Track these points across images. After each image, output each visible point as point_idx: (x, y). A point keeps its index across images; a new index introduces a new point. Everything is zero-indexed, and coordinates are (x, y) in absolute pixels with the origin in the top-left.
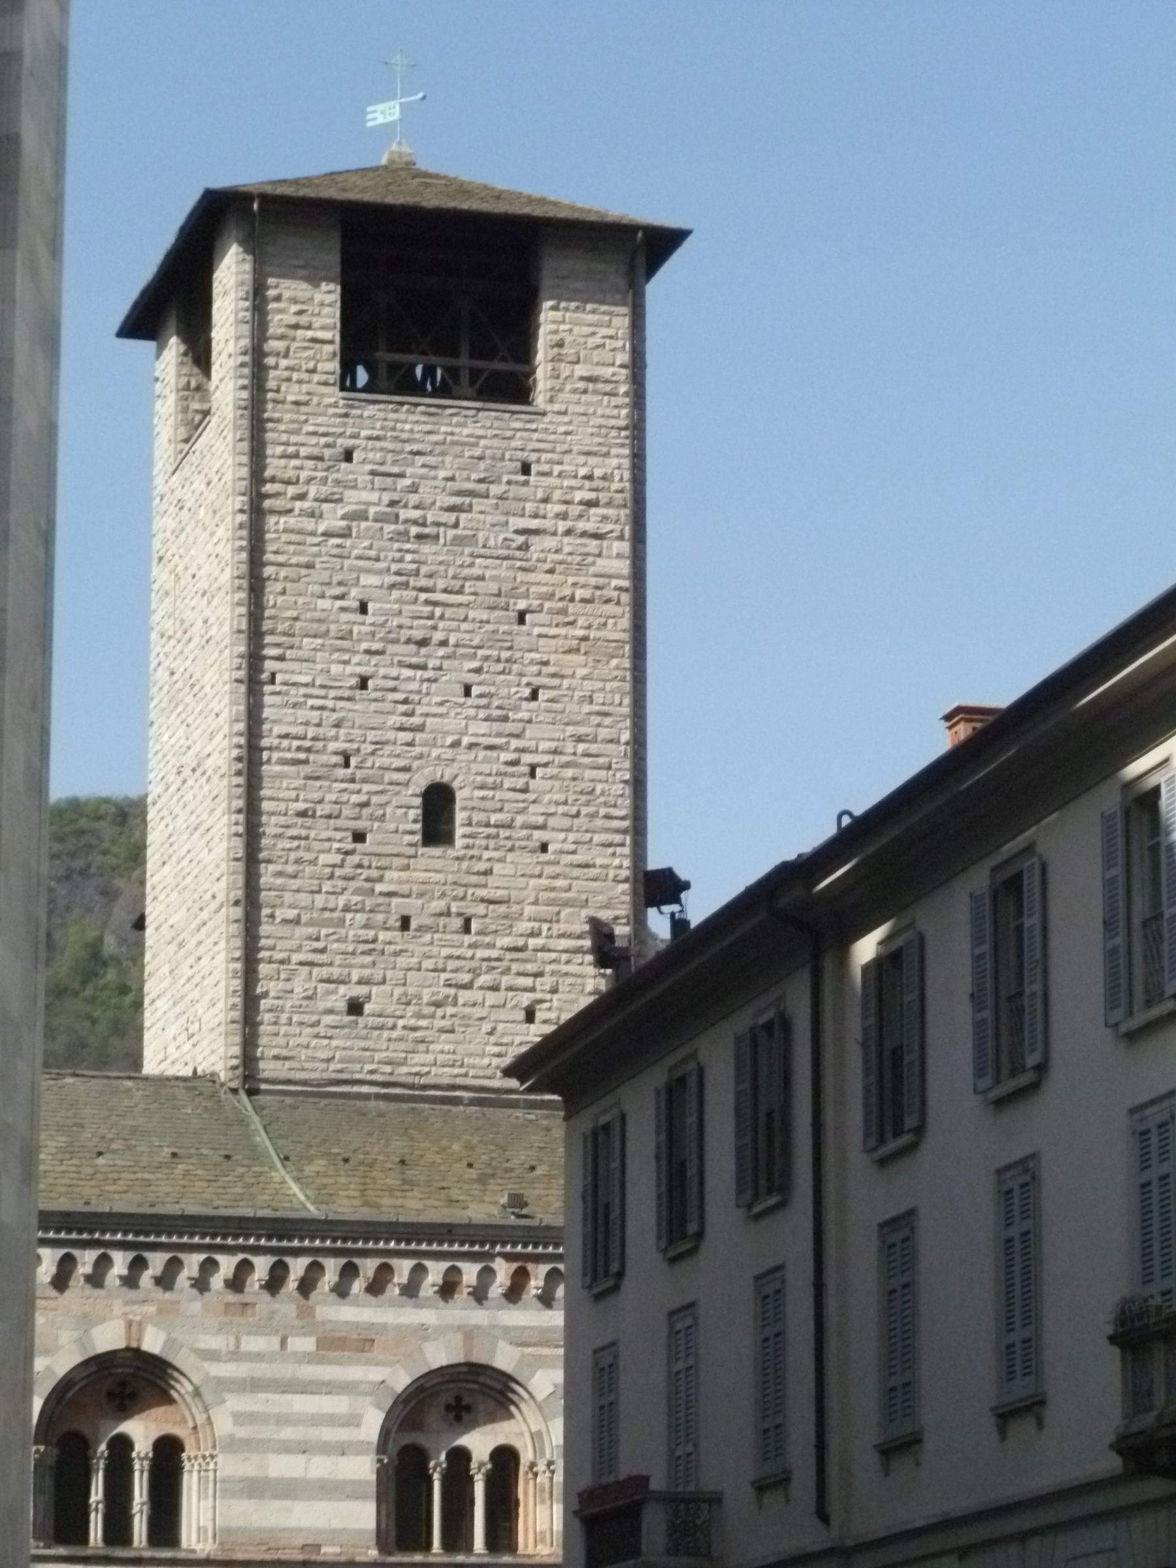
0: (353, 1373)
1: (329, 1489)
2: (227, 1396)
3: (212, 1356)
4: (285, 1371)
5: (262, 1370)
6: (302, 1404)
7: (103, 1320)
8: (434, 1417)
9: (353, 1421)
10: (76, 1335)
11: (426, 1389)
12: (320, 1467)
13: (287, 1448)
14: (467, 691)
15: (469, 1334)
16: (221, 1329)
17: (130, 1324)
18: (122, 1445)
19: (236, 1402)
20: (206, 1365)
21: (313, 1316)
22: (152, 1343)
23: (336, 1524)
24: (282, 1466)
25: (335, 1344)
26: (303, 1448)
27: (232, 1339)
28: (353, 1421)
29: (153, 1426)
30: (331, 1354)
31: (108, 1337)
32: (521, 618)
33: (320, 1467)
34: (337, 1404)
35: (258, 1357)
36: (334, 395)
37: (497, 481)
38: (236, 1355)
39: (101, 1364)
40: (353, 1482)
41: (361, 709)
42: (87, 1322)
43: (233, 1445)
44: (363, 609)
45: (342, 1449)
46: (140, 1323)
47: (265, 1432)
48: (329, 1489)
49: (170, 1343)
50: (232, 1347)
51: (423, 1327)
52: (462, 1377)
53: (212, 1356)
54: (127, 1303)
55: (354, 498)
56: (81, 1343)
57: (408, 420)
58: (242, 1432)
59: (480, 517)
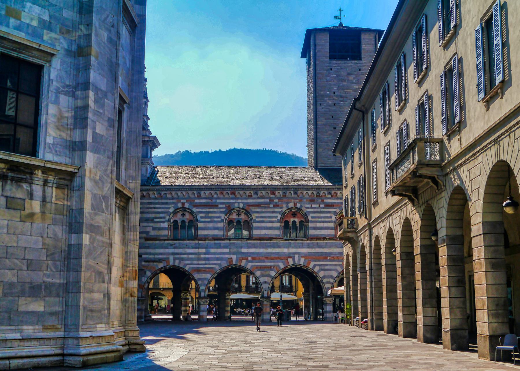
4: (319, 210)
5: (316, 210)
6: (322, 215)
7: (290, 203)
9: (331, 217)
12: (326, 225)
13: (320, 222)
16: (309, 204)
17: (294, 203)
18: (294, 222)
19: (312, 215)
22: (298, 206)
23: (329, 234)
24: (319, 225)
25: (328, 206)
28: (331, 217)
31: (291, 205)
33: (326, 225)
34: (328, 215)
35: (315, 208)
36: (328, 59)
37: (355, 71)
38: (312, 208)
39: (291, 209)
41: (333, 108)
42: (288, 203)
44: (334, 93)
45: (329, 222)
47: (317, 220)
49: (301, 206)
55: (332, 76)
56: (287, 206)
57: (341, 62)
58: (313, 220)
59: (351, 78)
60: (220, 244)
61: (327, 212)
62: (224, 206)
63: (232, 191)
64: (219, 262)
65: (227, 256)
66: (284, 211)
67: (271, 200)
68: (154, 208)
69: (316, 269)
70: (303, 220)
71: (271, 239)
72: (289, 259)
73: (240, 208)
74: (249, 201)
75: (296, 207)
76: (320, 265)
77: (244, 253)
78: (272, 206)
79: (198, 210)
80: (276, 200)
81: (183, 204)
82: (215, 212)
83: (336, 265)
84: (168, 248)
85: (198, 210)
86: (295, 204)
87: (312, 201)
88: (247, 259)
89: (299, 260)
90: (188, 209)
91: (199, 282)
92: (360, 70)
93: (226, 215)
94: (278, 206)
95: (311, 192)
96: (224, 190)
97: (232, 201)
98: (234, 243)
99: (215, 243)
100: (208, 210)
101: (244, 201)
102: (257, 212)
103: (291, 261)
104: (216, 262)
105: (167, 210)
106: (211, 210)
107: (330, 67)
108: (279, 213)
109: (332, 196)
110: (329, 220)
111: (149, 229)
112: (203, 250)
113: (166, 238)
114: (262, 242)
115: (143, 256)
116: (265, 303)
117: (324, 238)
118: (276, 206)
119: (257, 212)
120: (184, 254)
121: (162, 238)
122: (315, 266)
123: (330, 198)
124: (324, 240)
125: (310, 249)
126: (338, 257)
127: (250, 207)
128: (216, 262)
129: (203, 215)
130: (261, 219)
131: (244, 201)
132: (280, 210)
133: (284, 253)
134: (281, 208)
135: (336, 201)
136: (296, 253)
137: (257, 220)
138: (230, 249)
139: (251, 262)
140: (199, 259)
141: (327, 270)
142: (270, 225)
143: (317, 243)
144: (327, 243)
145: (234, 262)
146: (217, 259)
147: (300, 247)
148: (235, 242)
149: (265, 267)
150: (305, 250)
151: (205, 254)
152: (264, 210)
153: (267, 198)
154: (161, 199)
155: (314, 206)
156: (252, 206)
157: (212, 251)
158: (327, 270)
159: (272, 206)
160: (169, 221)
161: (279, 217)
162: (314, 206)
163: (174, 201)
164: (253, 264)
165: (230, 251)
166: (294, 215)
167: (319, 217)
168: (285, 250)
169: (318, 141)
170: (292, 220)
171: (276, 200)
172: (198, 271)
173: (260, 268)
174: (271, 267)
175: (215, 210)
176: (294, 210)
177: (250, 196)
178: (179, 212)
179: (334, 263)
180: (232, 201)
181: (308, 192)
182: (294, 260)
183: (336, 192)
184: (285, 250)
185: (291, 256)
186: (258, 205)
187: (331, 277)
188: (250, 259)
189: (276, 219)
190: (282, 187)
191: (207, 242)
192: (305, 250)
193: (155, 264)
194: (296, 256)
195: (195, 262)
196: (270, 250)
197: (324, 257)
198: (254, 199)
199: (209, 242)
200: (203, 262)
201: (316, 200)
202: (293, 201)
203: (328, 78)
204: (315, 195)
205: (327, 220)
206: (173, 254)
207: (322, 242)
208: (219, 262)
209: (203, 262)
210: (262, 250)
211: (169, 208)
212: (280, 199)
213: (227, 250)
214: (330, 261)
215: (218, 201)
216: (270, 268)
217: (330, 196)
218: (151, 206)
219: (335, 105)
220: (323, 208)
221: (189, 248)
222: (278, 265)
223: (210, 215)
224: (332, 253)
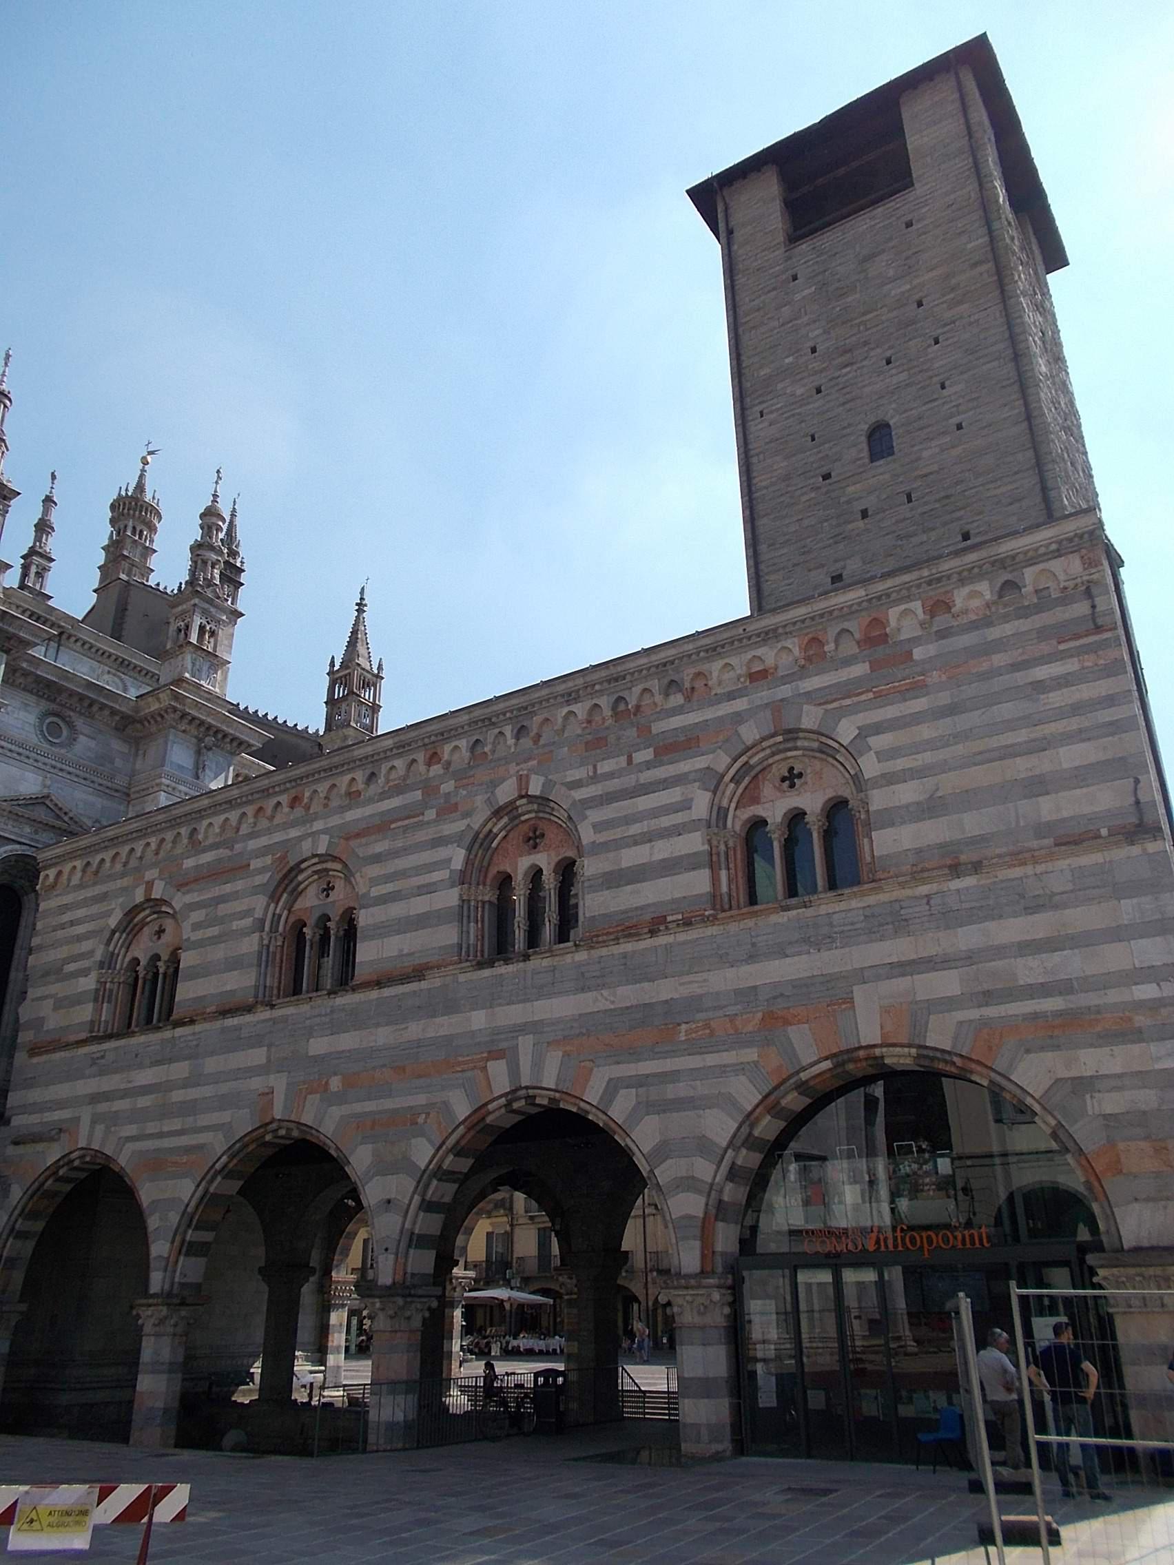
0: (685, 766)
1: (669, 867)
2: (588, 812)
3: (577, 784)
4: (629, 781)
5: (614, 785)
7: (504, 780)
8: (767, 790)
9: (686, 805)
10: (486, 797)
11: (752, 767)
13: (636, 841)
14: (889, 362)
15: (776, 707)
17: (520, 778)
19: (595, 816)
20: (573, 793)
21: (650, 732)
22: (535, 788)
23: (678, 895)
24: (631, 857)
26: (648, 838)
27: (591, 768)
28: (686, 805)
29: (553, 853)
30: (665, 758)
31: (506, 792)
32: (920, 304)
35: (611, 775)
38: (595, 778)
40: (688, 855)
42: (494, 784)
43: (599, 848)
45: (677, 831)
46: (527, 776)
48: (669, 867)
49: (548, 784)
50: (591, 774)
51: (738, 714)
52: (781, 747)
53: (577, 784)
54: (518, 764)
58: (601, 838)
60: (238, 1028)
61: (665, 784)
62: (268, 860)
63: (293, 793)
64: (225, 1117)
65: (257, 1083)
66: (476, 827)
67: (429, 789)
68: (72, 923)
69: (619, 1111)
70: (571, 853)
71: (418, 973)
73: (323, 858)
74: (351, 815)
75: (527, 796)
76: (640, 1082)
77: (316, 1059)
78: (431, 814)
79: (190, 898)
80: (447, 787)
81: (150, 885)
82: (235, 896)
83: (723, 1070)
84: (83, 1077)
85: (190, 898)
86: (523, 781)
87: (596, 744)
89: (538, 1065)
90: (163, 901)
91: (153, 1223)
92: (909, 224)
93: (274, 897)
94: (455, 808)
95: (588, 704)
96: (269, 795)
97: (294, 833)
98: (285, 1019)
99: (223, 1030)
100: (216, 891)
101: (335, 821)
102: (377, 859)
103: (499, 1078)
105: (101, 922)
106: (228, 888)
107: (790, 273)
108: (457, 839)
109: (688, 699)
110: (679, 818)
111: (46, 1008)
112: (180, 1070)
113: (83, 1036)
114: (387, 992)
115: (16, 1121)
117: (657, 925)
118: (449, 809)
119: (377, 859)
120: (125, 1094)
121: (73, 1038)
123: (678, 711)
124: (653, 933)
125: (590, 995)
126: (732, 1018)
127: (353, 843)
129: (197, 916)
130: (389, 888)
131: (335, 821)
132: (460, 825)
133: (473, 1034)
134: (467, 815)
135: (709, 714)
136: (522, 1029)
137: (375, 892)
138: (270, 1046)
139: (340, 1098)
140: (165, 1112)
141: (680, 1104)
142: (420, 905)
143: (625, 956)
144: (668, 948)
146: (224, 1102)
147: (543, 992)
148: (290, 1010)
150: (561, 1007)
151: (186, 1084)
152: (399, 844)
153: (411, 788)
154: (95, 884)
155: (605, 767)
156: (358, 835)
157: (211, 1065)
158: (680, 1104)
159: (431, 814)
160: (108, 962)
161: (458, 857)
162: (605, 767)
163: (126, 882)
164: (345, 1110)
165: (269, 1060)
166: (534, 840)
167: (628, 820)
168: (479, 1020)
169: (763, 548)
170: (521, 866)
171: (447, 787)
172: (157, 1165)
175: (239, 885)
176: (528, 812)
177: (353, 797)
178: (143, 924)
179: (711, 1060)
180: (294, 833)
181: (573, 708)
182: (514, 1071)
183: (704, 667)
184: (479, 1020)
185: (498, 1048)
186: (381, 827)
187: (702, 1146)
188: (335, 1083)
189: (443, 874)
190: (465, 718)
191: (197, 1028)
192: (561, 1007)
193: (40, 1147)
194: (525, 1043)
195: (151, 1128)
196: (415, 1030)
197: (658, 1027)
198: (371, 801)
199: (207, 1026)
200: (176, 1124)
201: (612, 738)
202: (513, 768)
203: (786, 311)
204: (607, 712)
205: (666, 821)
206: (95, 1098)
207: (648, 943)
208: (225, 1117)
209: (176, 1124)
210: (383, 1036)
211: (108, 914)
212: (461, 776)
213: (258, 1056)
214: (694, 1048)
215: (253, 844)
216: (408, 1122)
217: (677, 699)
218: (66, 918)
219: (819, 391)
220: (648, 765)
221: (141, 1066)
222: (446, 1107)
223: (223, 909)
224: (701, 996)
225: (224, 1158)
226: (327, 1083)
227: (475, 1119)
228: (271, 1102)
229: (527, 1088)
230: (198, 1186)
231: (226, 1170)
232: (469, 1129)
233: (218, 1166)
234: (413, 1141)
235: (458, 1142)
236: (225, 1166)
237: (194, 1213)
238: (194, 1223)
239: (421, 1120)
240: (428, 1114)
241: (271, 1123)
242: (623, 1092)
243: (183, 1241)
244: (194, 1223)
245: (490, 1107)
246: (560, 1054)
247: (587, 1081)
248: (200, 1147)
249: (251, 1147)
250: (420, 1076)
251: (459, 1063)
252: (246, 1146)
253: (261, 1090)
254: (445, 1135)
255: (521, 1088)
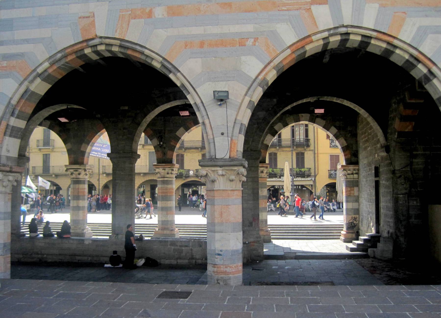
64: (45, 33)
72: (314, 8)
88: (150, 15)
89: (358, 10)
104: (36, 33)
116: (221, 184)
122: (423, 32)
128: (36, 33)
145: (101, 29)
149: (222, 42)
173: (202, 45)
174: (242, 44)
188: (159, 12)
208: (45, 33)
225: (46, 65)
226: (151, 11)
227: (300, 45)
228: (93, 24)
229: (347, 27)
230: (21, 85)
231: (46, 74)
232: (293, 52)
233: (40, 70)
234: (243, 58)
235: (281, 62)
236: (45, 71)
237: (16, 105)
238: (17, 112)
239: (250, 42)
240: (256, 39)
241: (93, 39)
242: (430, 36)
243: (8, 125)
244: (17, 112)
245: (314, 38)
246: (377, 5)
247: (401, 26)
248: (22, 55)
249: (70, 58)
250: (246, 11)
251: (285, 5)
252: (66, 56)
253: (83, 15)
254: (274, 55)
255: (343, 26)
